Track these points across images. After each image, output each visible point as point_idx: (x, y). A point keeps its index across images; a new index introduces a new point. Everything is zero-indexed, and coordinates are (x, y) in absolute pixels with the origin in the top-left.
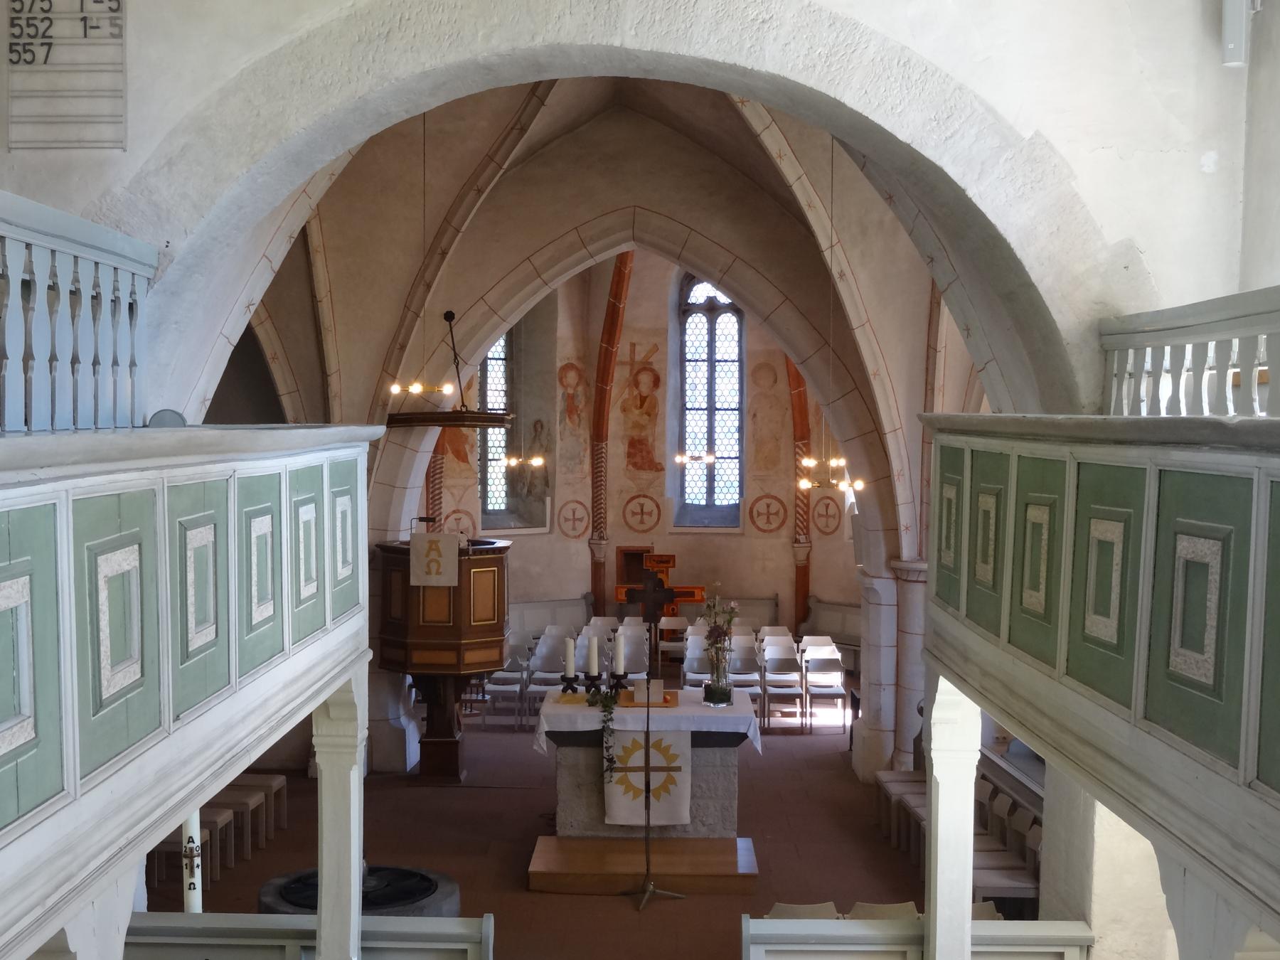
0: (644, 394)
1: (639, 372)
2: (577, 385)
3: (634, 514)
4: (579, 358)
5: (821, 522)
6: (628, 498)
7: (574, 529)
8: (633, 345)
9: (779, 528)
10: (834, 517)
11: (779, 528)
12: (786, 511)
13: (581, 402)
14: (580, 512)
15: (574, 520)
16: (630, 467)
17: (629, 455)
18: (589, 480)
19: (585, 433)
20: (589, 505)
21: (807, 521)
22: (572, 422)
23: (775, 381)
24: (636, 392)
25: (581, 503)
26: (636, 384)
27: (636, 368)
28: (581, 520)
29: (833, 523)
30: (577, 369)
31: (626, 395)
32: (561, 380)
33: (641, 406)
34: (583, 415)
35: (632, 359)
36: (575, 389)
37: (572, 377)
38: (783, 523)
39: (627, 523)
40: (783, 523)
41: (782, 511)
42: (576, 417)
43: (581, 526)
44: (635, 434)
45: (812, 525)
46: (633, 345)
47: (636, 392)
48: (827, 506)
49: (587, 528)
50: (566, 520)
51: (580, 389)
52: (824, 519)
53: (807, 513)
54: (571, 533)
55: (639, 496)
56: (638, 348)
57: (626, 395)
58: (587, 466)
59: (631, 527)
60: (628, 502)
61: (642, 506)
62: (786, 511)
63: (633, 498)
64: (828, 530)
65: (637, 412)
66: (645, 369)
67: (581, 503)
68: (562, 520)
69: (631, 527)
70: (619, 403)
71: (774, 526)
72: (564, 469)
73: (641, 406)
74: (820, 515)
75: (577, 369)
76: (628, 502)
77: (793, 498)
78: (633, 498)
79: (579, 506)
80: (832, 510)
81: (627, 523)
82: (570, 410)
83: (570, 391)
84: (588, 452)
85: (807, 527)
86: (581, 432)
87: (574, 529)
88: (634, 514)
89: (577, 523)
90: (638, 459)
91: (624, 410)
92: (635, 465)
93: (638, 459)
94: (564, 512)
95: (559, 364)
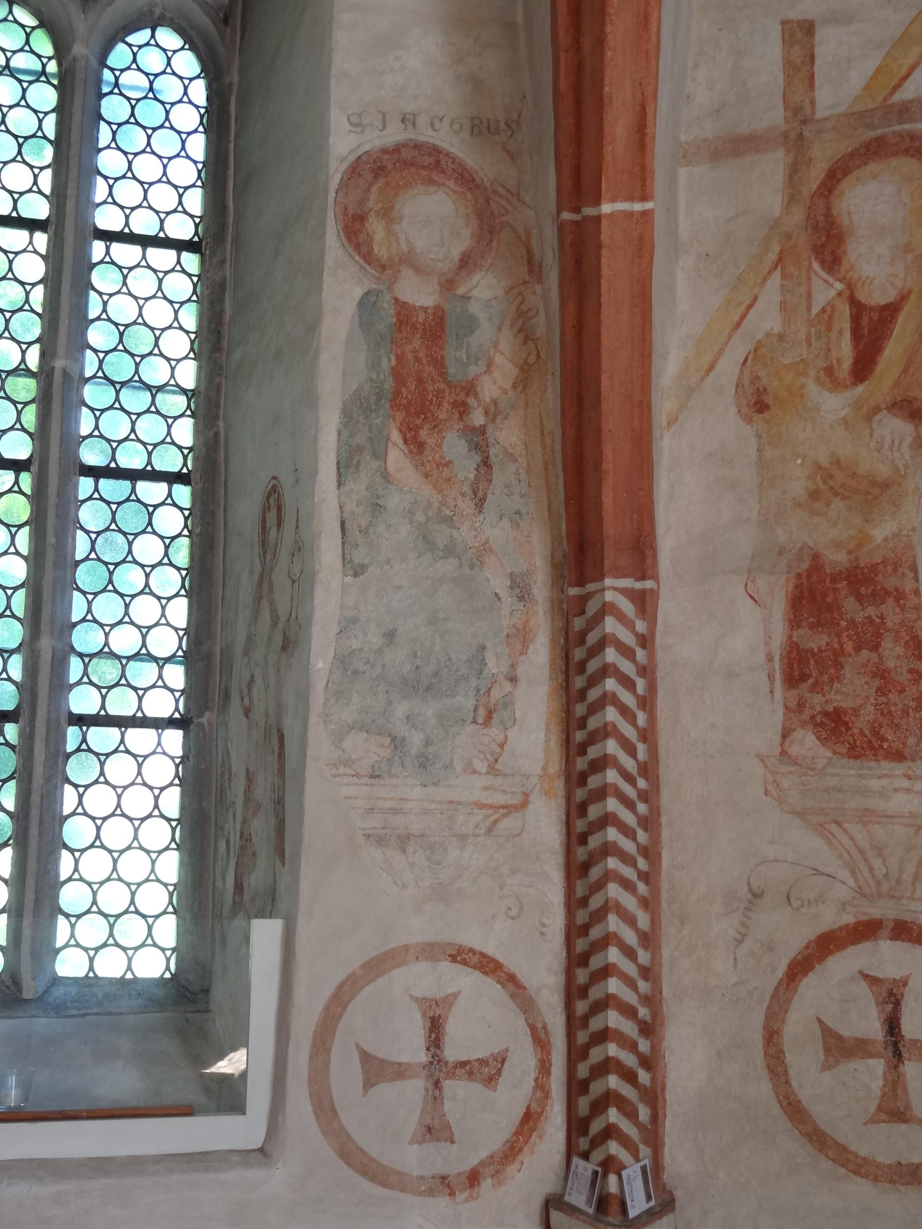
0: (877, 295)
1: (836, 175)
2: (466, 263)
3: (838, 1048)
4: (480, 128)
6: (796, 938)
7: (435, 1130)
8: (800, 34)
13: (491, 360)
14: (481, 1022)
15: (438, 1069)
16: (806, 742)
17: (797, 668)
18: (545, 823)
19: (516, 540)
20: (544, 974)
22: (435, 471)
24: (825, 291)
25: (488, 966)
26: (828, 242)
27: (823, 154)
28: (487, 1071)
30: (466, 179)
31: (766, 319)
32: (354, 229)
33: (863, 368)
34: (508, 435)
35: (800, 114)
36: (448, 285)
37: (430, 222)
39: (795, 1110)
42: (454, 446)
43: (483, 1117)
44: (831, 535)
46: (800, 34)
47: (825, 291)
49: (529, 1121)
50: (375, 1070)
51: (485, 289)
54: (414, 1159)
55: (866, 931)
56: (829, 44)
57: (766, 319)
58: (532, 735)
59: (819, 1139)
60: (800, 968)
61: (892, 998)
63: (827, 944)
65: (833, 404)
66: (875, 150)
67: (488, 966)
68: (345, 1073)
69: (819, 1139)
70: (728, 368)
72: (365, 749)
73: (863, 368)
75: (466, 179)
76: (800, 968)
78: (827, 944)
79: (465, 981)
81: (795, 1110)
82: (418, 388)
83: (420, 294)
84: (540, 654)
86: (495, 530)
87: (435, 1130)
88: (838, 1048)
89: (460, 1094)
90: (852, 690)
91: (759, 404)
92: (834, 726)
93: (852, 690)
94: (357, 1023)
95: (344, 143)
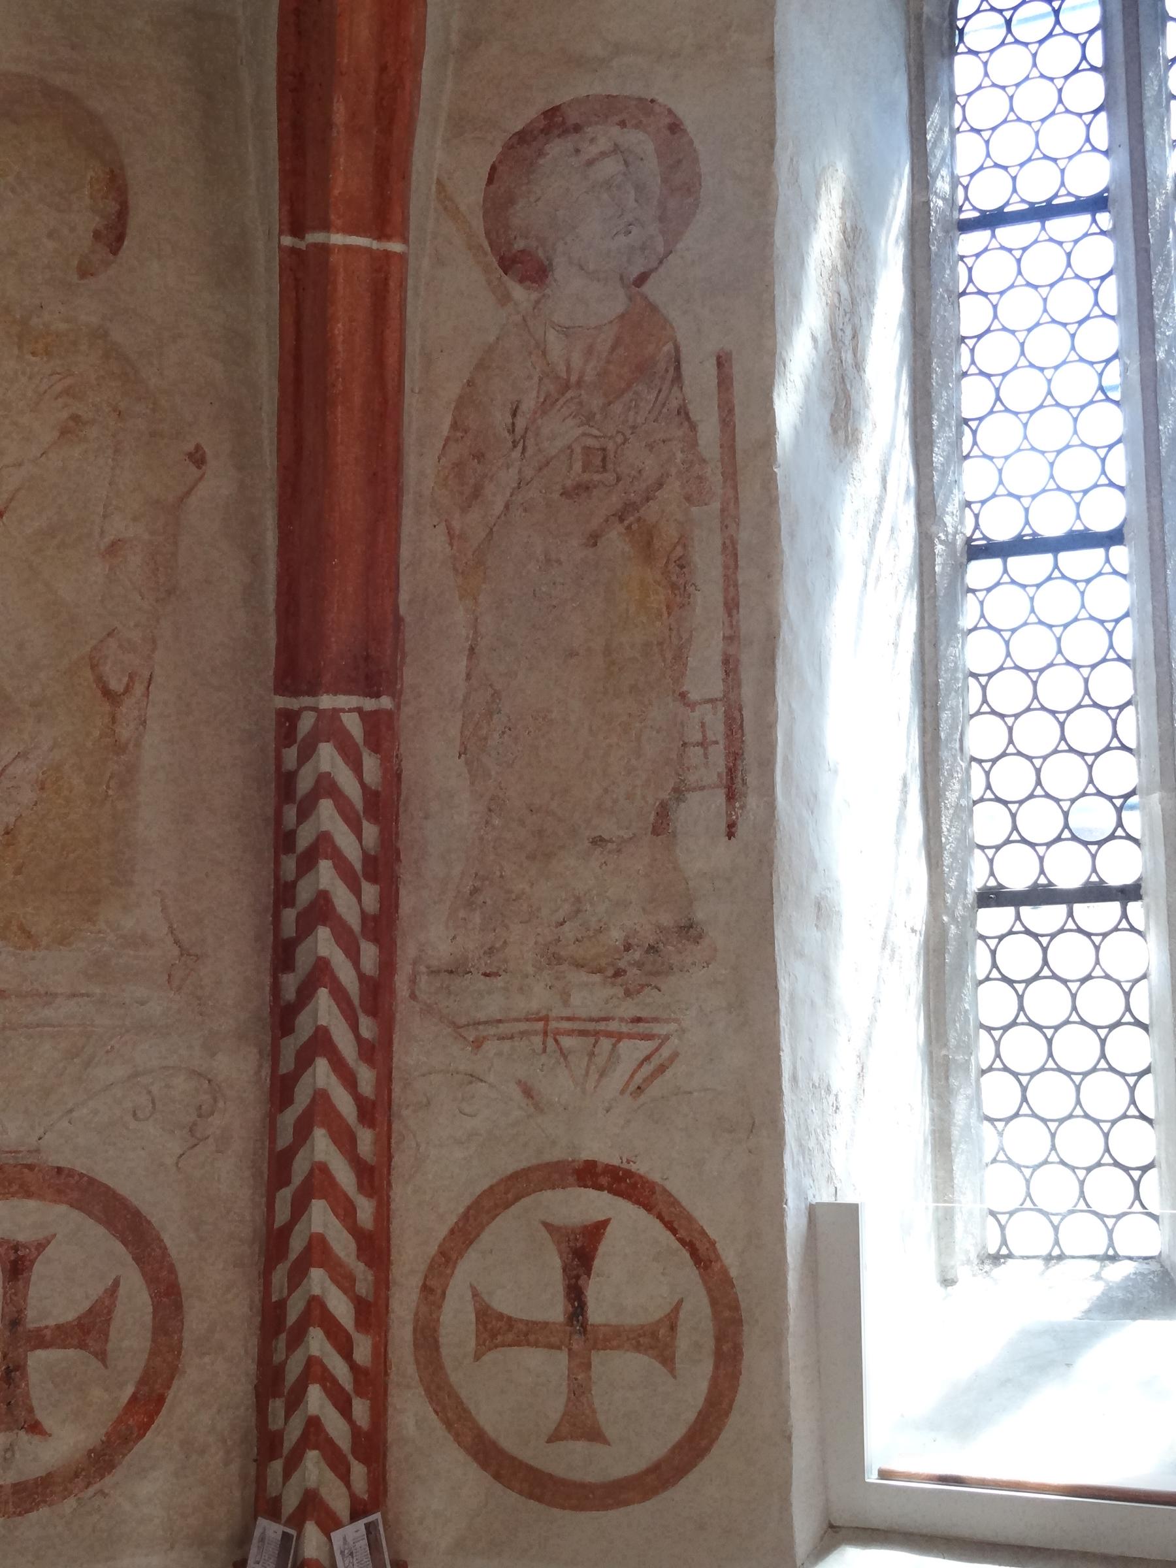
5: (516, 1394)
9: (101, 1461)
10: (656, 1341)
11: (101, 1461)
12: (168, 1296)
21: (373, 1382)
23: (114, 235)
29: (641, 1406)
38: (146, 1405)
40: (146, 1405)
41: (136, 1304)
45: (410, 1413)
48: (581, 1250)
52: (541, 1369)
53: (372, 1313)
62: (168, 1296)
64: (574, 1461)
71: (64, 1441)
74: (495, 1330)
77: (231, 1178)
80: (637, 1274)
85: (372, 1446)
